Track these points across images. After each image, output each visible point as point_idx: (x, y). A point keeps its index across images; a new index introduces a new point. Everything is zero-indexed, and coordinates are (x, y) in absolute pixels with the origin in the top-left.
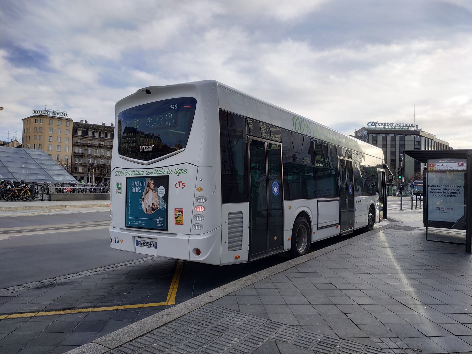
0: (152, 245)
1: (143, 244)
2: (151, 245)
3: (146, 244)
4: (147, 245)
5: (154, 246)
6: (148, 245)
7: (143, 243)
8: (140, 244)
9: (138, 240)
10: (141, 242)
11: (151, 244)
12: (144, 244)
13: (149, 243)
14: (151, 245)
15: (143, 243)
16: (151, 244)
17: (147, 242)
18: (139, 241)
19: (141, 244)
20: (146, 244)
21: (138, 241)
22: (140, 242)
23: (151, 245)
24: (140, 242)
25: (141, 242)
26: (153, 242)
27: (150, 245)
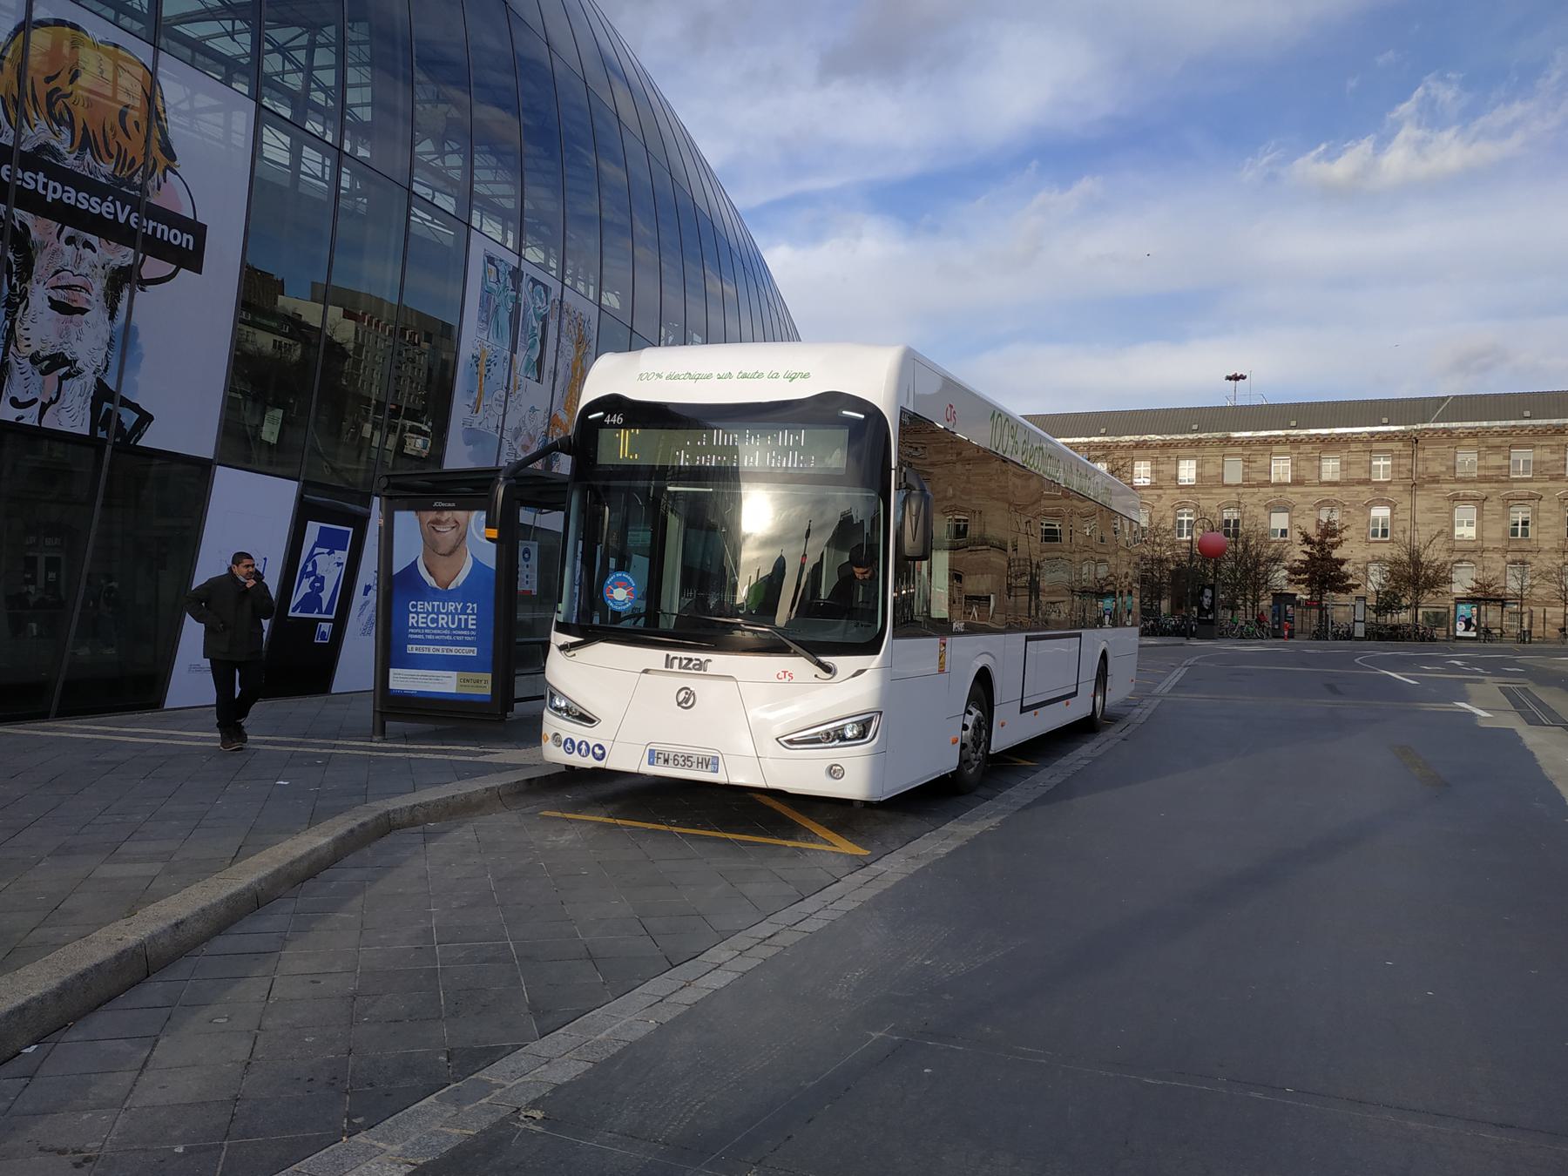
0: (702, 763)
1: (671, 762)
2: (698, 763)
3: (684, 761)
4: (687, 763)
5: (709, 766)
6: (689, 763)
7: (671, 757)
8: (662, 760)
9: (654, 750)
10: (666, 756)
11: (700, 761)
12: (675, 760)
13: (694, 759)
14: (700, 765)
15: (671, 757)
16: (700, 761)
17: (686, 755)
18: (658, 753)
19: (666, 761)
20: (684, 761)
21: (656, 752)
22: (660, 756)
23: (700, 765)
24: (660, 756)
25: (666, 756)
26: (707, 758)
27: (695, 765)
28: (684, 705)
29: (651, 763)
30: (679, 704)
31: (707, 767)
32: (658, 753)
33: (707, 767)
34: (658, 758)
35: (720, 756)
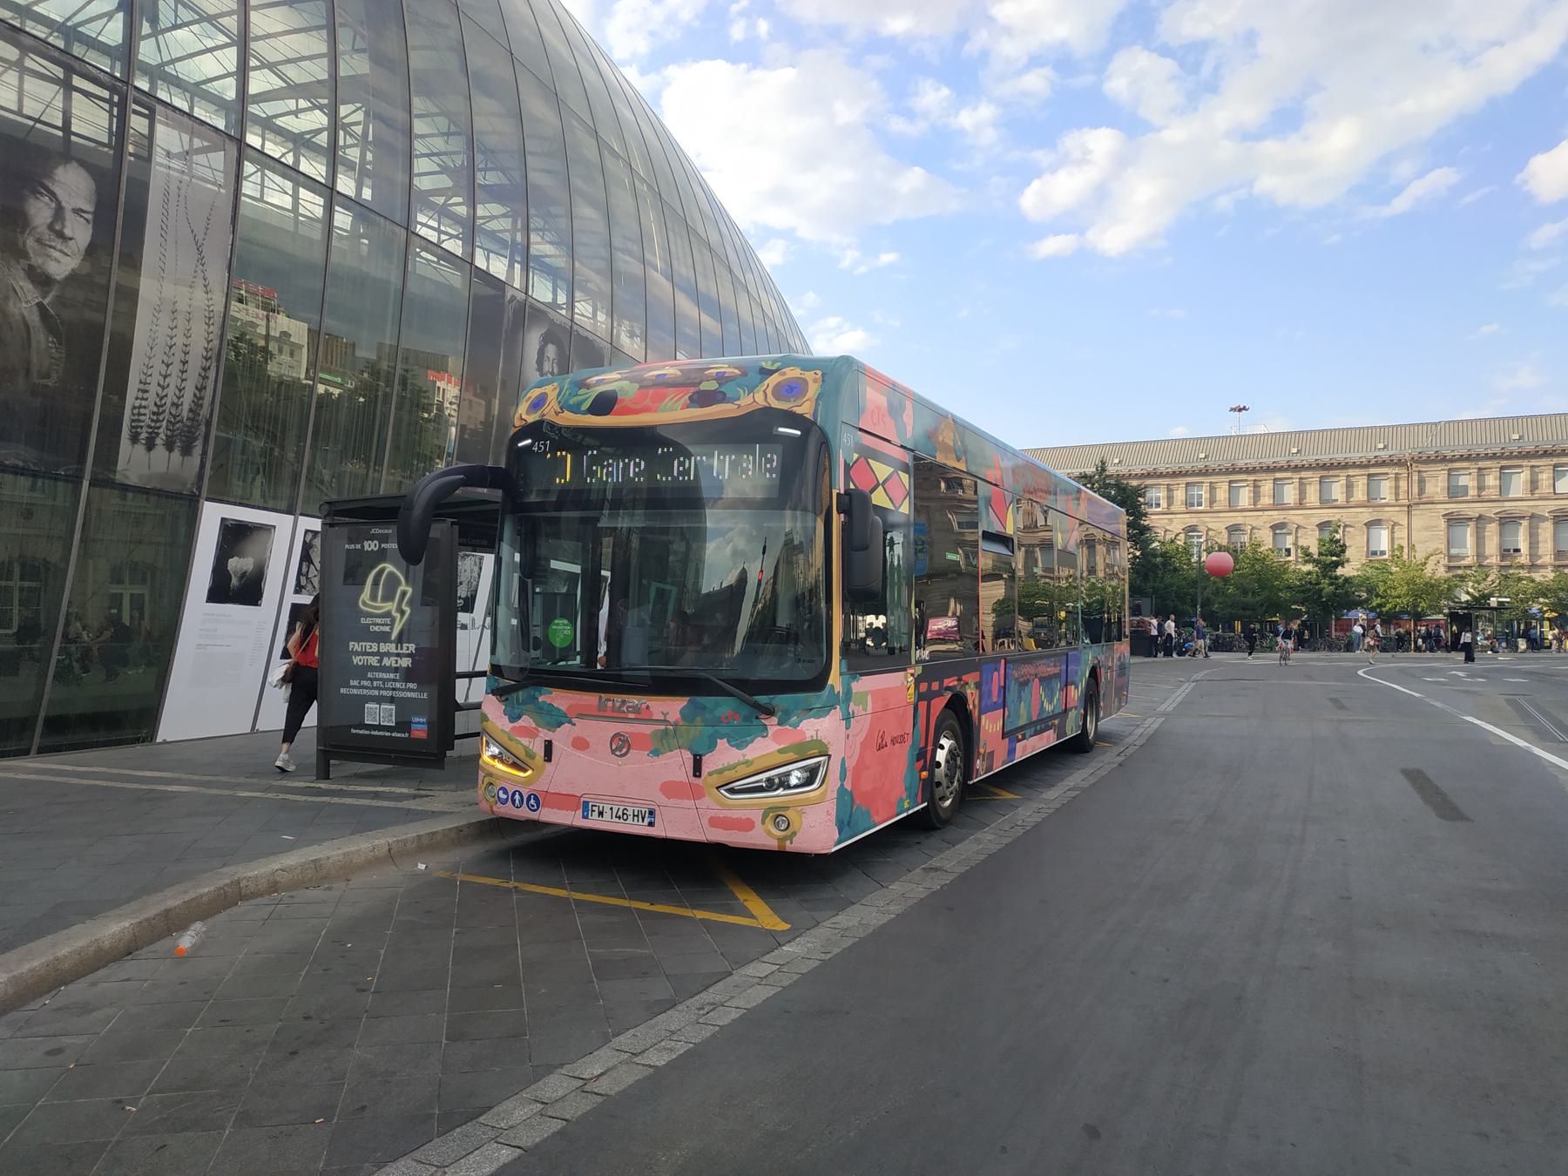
0: (638, 816)
2: (634, 816)
5: (646, 819)
8: (596, 813)
10: (601, 809)
11: (636, 814)
14: (636, 818)
16: (636, 814)
18: (592, 806)
21: (590, 804)
22: (594, 808)
23: (636, 818)
24: (594, 808)
25: (601, 809)
26: (643, 810)
28: (618, 753)
29: (585, 817)
30: (613, 752)
31: (643, 821)
32: (592, 806)
33: (643, 821)
34: (593, 811)
35: (657, 808)
